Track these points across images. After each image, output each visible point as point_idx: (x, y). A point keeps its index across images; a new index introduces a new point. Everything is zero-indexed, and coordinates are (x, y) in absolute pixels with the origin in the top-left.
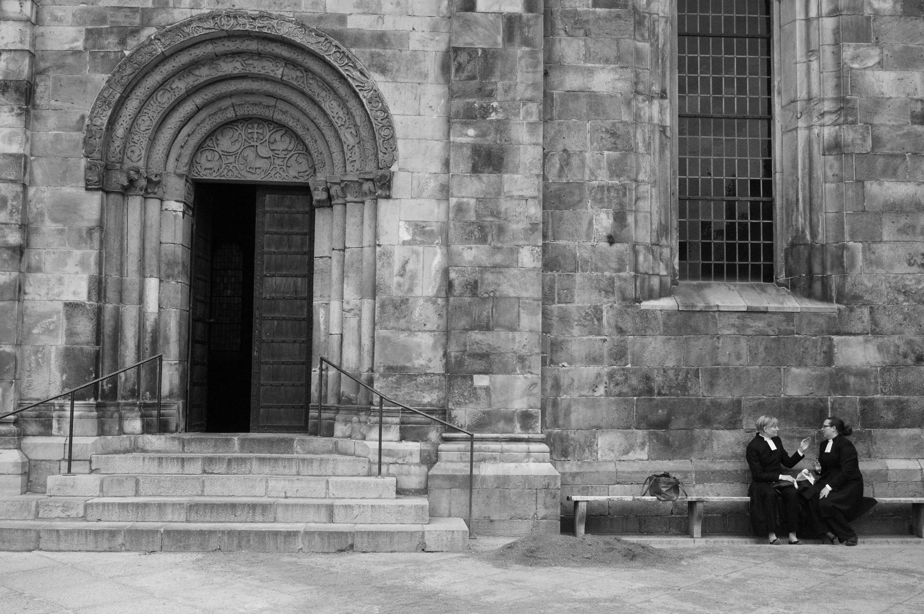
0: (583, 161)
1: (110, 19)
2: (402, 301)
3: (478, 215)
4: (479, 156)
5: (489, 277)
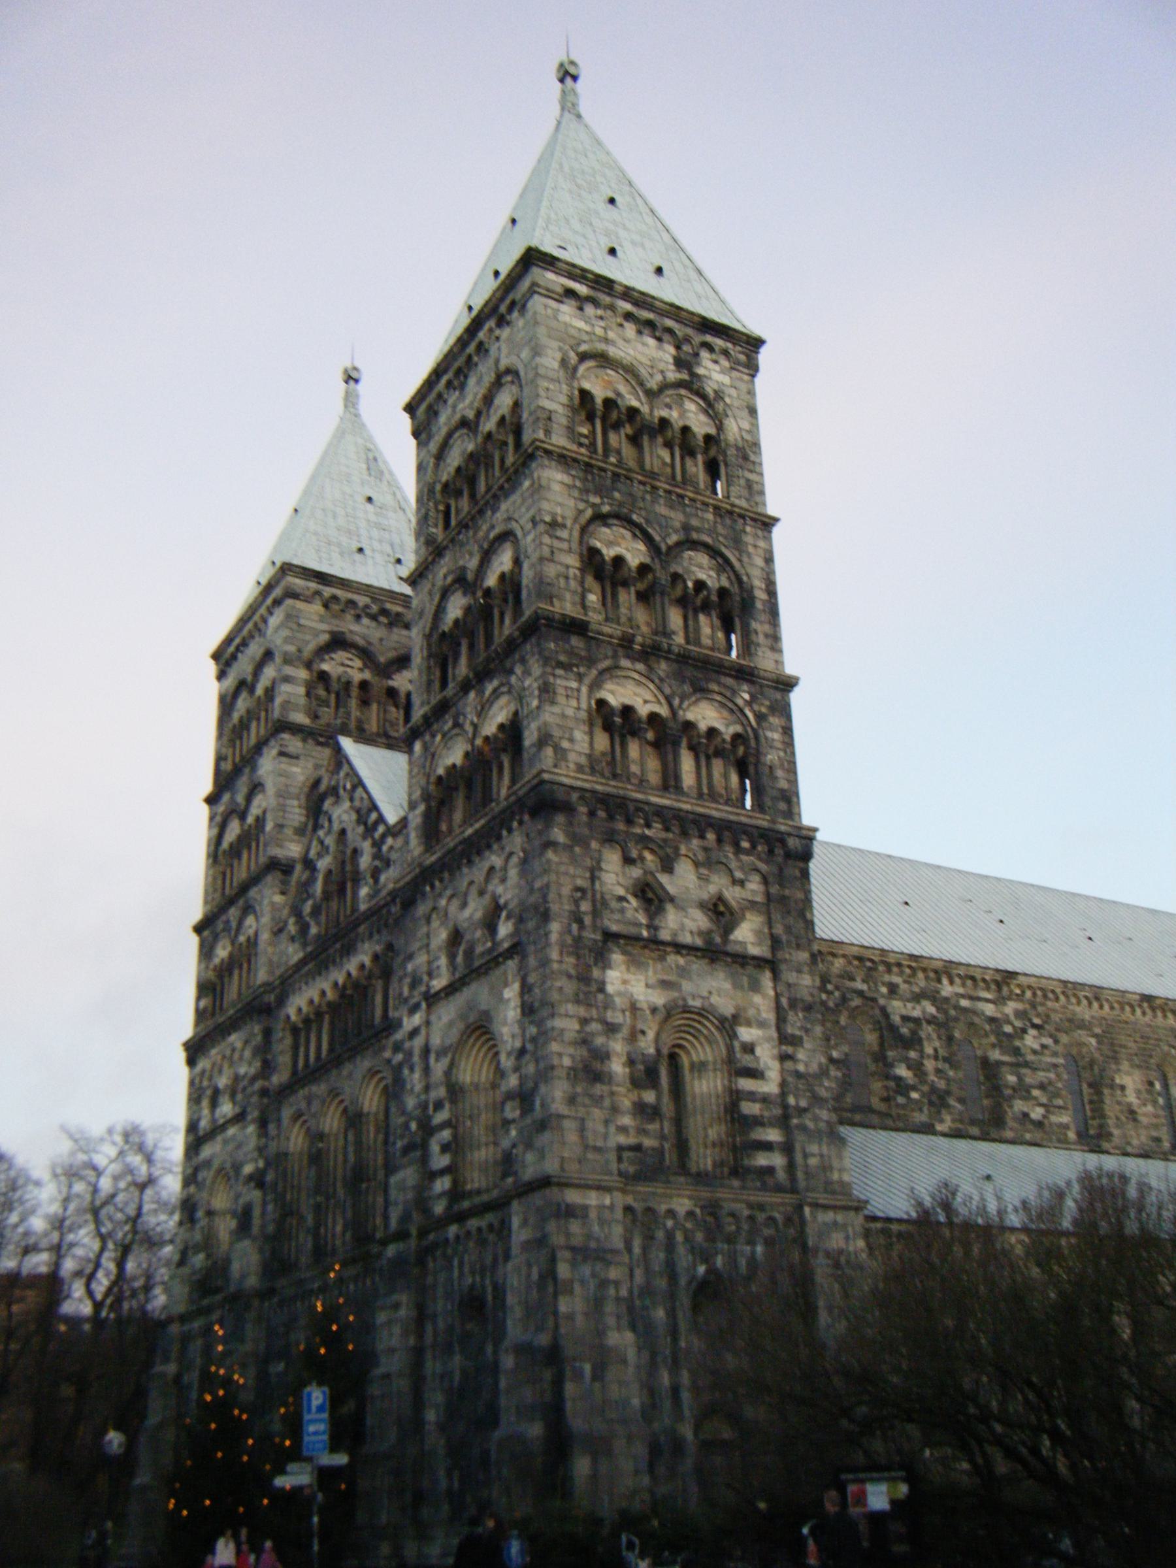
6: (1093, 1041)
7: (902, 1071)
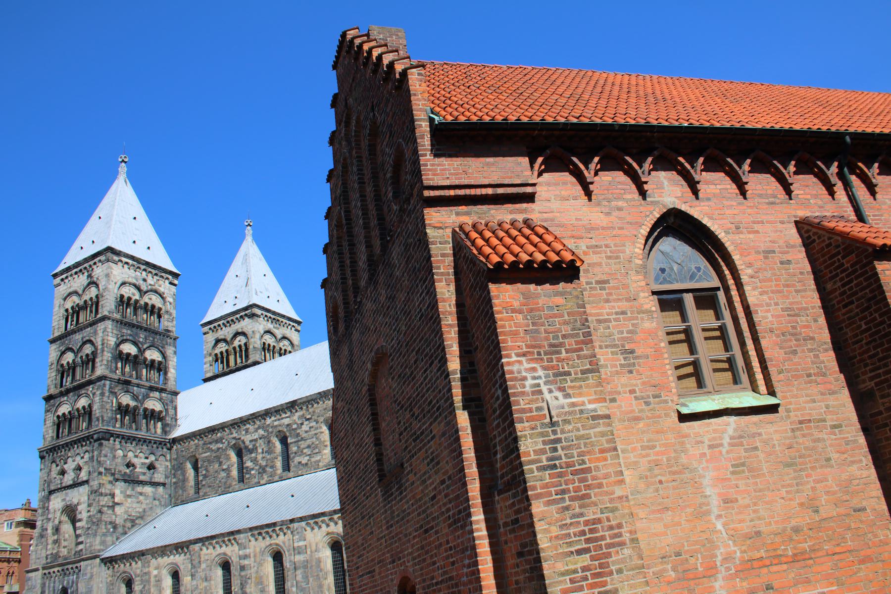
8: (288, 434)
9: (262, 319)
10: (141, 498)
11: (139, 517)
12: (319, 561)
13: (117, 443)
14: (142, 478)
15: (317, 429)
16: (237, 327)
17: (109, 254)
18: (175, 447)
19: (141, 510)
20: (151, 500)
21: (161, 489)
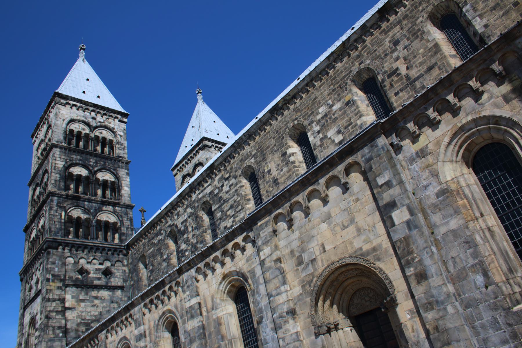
0: (461, 259)
1: (305, 280)
2: (417, 342)
3: (427, 299)
4: (418, 277)
5: (441, 322)
6: (253, 160)
7: (183, 246)
8: (211, 202)
9: (213, 149)
10: (96, 302)
11: (95, 321)
12: (218, 323)
13: (66, 251)
14: (96, 282)
15: (236, 184)
16: (195, 161)
17: (57, 99)
18: (130, 252)
19: (97, 313)
20: (108, 304)
21: (119, 293)
